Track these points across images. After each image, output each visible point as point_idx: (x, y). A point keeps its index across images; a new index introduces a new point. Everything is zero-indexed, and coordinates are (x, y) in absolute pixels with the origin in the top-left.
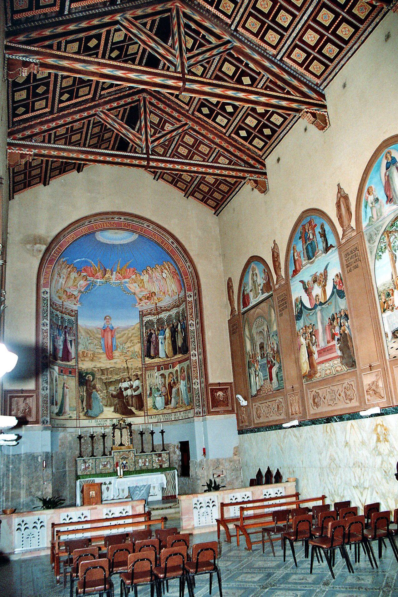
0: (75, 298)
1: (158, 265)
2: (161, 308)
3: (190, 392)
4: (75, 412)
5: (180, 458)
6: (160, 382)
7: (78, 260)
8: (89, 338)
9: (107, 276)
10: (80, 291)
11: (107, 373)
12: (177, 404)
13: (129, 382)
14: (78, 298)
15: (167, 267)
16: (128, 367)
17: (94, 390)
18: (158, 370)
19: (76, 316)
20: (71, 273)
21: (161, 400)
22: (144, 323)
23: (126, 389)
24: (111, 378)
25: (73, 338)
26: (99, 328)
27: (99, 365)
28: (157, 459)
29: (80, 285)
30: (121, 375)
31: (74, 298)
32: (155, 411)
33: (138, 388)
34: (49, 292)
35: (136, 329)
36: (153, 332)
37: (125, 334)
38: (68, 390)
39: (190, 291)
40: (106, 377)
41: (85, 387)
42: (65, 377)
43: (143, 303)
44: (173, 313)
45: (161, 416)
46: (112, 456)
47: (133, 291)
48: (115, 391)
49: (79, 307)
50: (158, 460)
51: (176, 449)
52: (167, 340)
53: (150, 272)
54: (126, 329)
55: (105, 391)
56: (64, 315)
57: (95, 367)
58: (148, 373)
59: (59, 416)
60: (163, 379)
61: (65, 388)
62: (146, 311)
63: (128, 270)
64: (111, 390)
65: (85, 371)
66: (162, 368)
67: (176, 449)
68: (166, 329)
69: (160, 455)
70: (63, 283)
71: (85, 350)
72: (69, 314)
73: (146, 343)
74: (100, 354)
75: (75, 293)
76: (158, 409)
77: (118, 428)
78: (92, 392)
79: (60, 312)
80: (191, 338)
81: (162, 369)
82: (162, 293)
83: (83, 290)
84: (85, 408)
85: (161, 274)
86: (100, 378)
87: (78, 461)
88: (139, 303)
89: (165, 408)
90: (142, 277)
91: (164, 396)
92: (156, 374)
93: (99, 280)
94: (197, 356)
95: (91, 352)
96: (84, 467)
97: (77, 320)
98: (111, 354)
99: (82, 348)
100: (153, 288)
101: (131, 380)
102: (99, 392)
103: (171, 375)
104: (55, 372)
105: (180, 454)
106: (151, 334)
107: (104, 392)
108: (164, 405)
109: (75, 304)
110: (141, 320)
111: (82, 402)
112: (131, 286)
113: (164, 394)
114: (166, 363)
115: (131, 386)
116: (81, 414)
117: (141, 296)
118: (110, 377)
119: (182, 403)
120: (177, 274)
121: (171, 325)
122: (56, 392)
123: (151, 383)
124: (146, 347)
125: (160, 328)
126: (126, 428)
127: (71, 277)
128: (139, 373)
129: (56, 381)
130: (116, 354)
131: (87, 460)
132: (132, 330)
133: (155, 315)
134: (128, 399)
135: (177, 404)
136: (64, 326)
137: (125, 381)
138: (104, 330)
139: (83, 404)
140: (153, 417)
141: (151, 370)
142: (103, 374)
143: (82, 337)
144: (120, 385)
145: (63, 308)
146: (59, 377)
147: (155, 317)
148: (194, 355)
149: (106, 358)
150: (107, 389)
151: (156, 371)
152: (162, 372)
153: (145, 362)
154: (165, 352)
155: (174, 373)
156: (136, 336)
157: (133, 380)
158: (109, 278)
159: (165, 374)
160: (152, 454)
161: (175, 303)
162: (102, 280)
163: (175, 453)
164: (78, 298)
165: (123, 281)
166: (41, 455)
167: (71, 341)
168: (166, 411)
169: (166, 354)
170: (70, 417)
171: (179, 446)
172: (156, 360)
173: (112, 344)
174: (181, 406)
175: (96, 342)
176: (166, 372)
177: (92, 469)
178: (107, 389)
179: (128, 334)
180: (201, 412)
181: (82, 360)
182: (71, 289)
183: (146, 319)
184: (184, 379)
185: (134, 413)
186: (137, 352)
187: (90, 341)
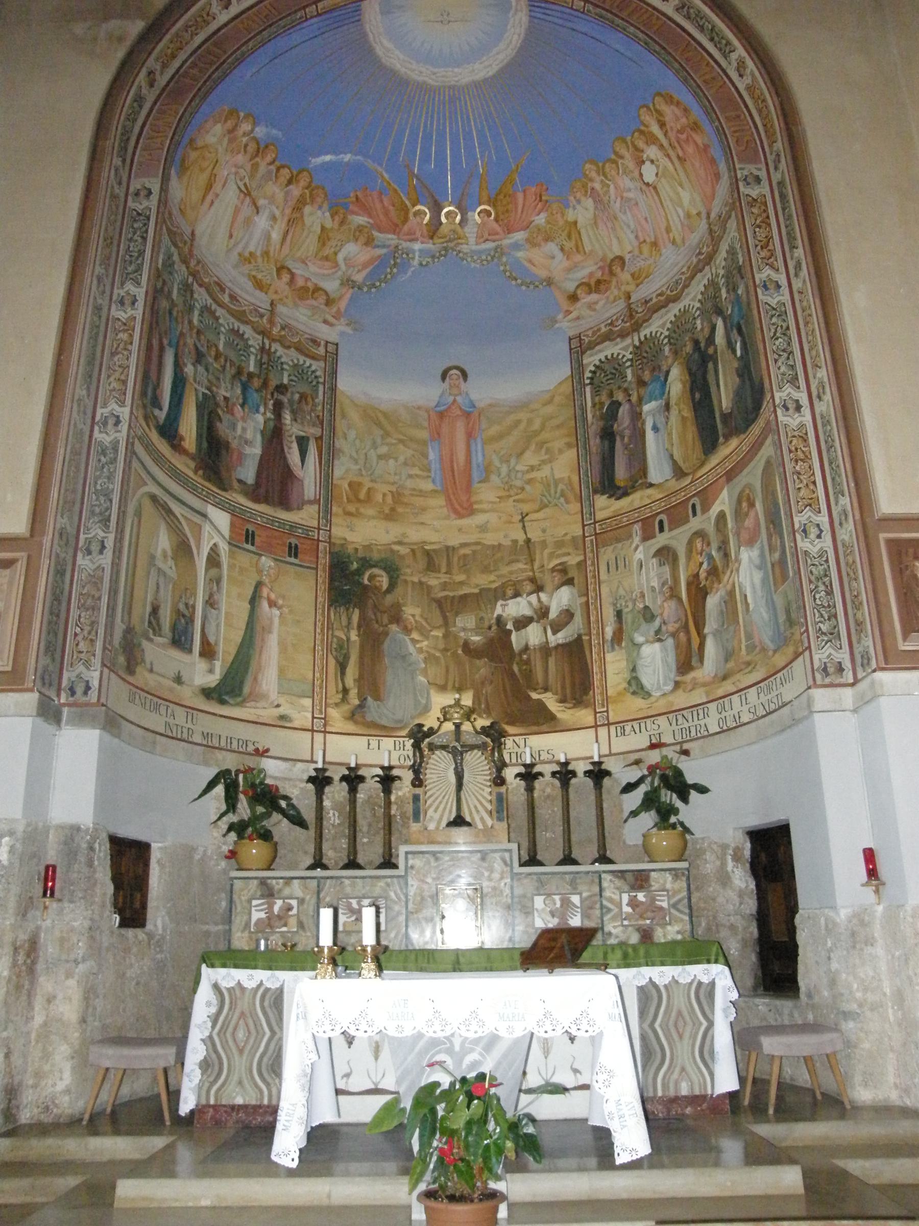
0: (329, 302)
1: (624, 141)
2: (646, 302)
3: (785, 577)
4: (307, 702)
5: (751, 905)
6: (655, 583)
7: (328, 158)
8: (379, 441)
9: (444, 230)
10: (348, 282)
11: (449, 564)
12: (726, 661)
13: (533, 598)
14: (343, 305)
15: (655, 129)
16: (528, 541)
17: (394, 628)
18: (647, 536)
19: (332, 357)
20: (307, 209)
21: (659, 656)
22: (589, 375)
23: (522, 623)
24: (462, 583)
25: (316, 431)
26: (419, 408)
27: (415, 535)
28: (625, 898)
29: (345, 259)
30: (505, 570)
31: (322, 299)
32: (637, 704)
33: (568, 615)
34: (156, 189)
35: (557, 399)
36: (620, 396)
37: (518, 423)
38: (276, 612)
39: (754, 159)
40: (444, 578)
41: (357, 611)
42: (266, 562)
43: (579, 309)
44: (693, 300)
45: (662, 721)
46: (401, 871)
47: (543, 274)
48: (477, 630)
49: (342, 334)
50: (633, 903)
51: (730, 864)
52: (674, 412)
53: (597, 186)
54: (523, 405)
55: (438, 633)
56: (275, 346)
57: (400, 543)
58: (607, 554)
59: (222, 702)
60: (667, 569)
61: (265, 604)
62: (594, 333)
63: (520, 196)
64: (464, 629)
65: (360, 554)
66: (661, 522)
67: (730, 864)
68: (668, 373)
69: (640, 880)
70: (276, 236)
71: (360, 479)
72: (297, 349)
73: (595, 443)
74: (422, 494)
75: (331, 286)
76: (647, 695)
77: (444, 747)
78: (386, 634)
79: (255, 330)
80: (775, 337)
81: (661, 529)
82: (646, 249)
83: (359, 278)
84: (353, 693)
85: (636, 174)
86: (421, 583)
87: (238, 884)
88: (568, 312)
89: (677, 685)
90: (571, 215)
91: (674, 635)
92: (639, 555)
93: (417, 246)
94: (806, 411)
95: (385, 488)
96: (263, 915)
97: (334, 373)
98: (464, 498)
99: (347, 471)
100: (615, 241)
101: (539, 589)
102: (415, 635)
103: (699, 544)
104: (207, 528)
105: (752, 885)
106: (616, 405)
107: (435, 633)
108: (673, 675)
109: (325, 322)
110: (575, 365)
111: (342, 667)
112: (536, 254)
113: (671, 627)
114: (674, 501)
115: (543, 612)
116: (334, 713)
117: (571, 286)
118: (461, 577)
119: (751, 648)
120: (695, 127)
121: (689, 348)
122: (211, 603)
123: (621, 592)
124: (596, 459)
125: (647, 376)
126: (482, 747)
127: (308, 220)
128: (573, 560)
129: (213, 561)
130: (486, 494)
131: (277, 885)
132: (544, 405)
133: (628, 335)
134: (528, 662)
135: (727, 660)
136: (273, 383)
137: (517, 595)
138: (441, 415)
139: (343, 673)
140: (628, 728)
141: (618, 540)
142: (431, 566)
143: (352, 434)
144: (498, 610)
145: (271, 322)
146: (232, 555)
147: (628, 341)
148: (791, 406)
149: (445, 510)
150: (446, 623)
151: (637, 540)
152: (661, 540)
153: (592, 514)
154: (672, 456)
155: (711, 529)
156: (558, 427)
157: (549, 587)
158: (457, 237)
159: (674, 544)
160: (599, 874)
161: (700, 253)
162: (429, 246)
163: (724, 879)
164: (343, 305)
165: (506, 242)
166: (11, 833)
167: (302, 442)
168: (681, 699)
169: (675, 463)
170: (282, 717)
171: (747, 853)
172: (637, 499)
173: (469, 461)
174: (748, 664)
175: (409, 453)
176: (677, 538)
177: (301, 925)
178: (446, 623)
179: (530, 422)
180: (847, 664)
181: (349, 514)
182: (313, 268)
183: (591, 360)
184: (751, 543)
185: (552, 717)
186: (561, 480)
187: (384, 450)
